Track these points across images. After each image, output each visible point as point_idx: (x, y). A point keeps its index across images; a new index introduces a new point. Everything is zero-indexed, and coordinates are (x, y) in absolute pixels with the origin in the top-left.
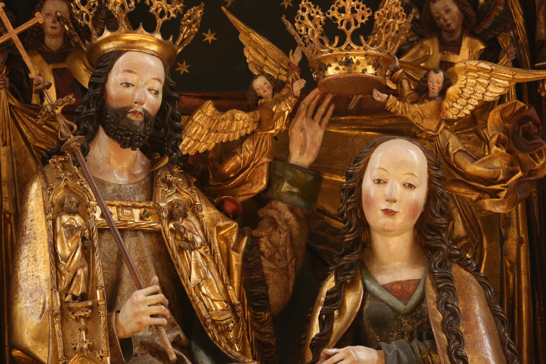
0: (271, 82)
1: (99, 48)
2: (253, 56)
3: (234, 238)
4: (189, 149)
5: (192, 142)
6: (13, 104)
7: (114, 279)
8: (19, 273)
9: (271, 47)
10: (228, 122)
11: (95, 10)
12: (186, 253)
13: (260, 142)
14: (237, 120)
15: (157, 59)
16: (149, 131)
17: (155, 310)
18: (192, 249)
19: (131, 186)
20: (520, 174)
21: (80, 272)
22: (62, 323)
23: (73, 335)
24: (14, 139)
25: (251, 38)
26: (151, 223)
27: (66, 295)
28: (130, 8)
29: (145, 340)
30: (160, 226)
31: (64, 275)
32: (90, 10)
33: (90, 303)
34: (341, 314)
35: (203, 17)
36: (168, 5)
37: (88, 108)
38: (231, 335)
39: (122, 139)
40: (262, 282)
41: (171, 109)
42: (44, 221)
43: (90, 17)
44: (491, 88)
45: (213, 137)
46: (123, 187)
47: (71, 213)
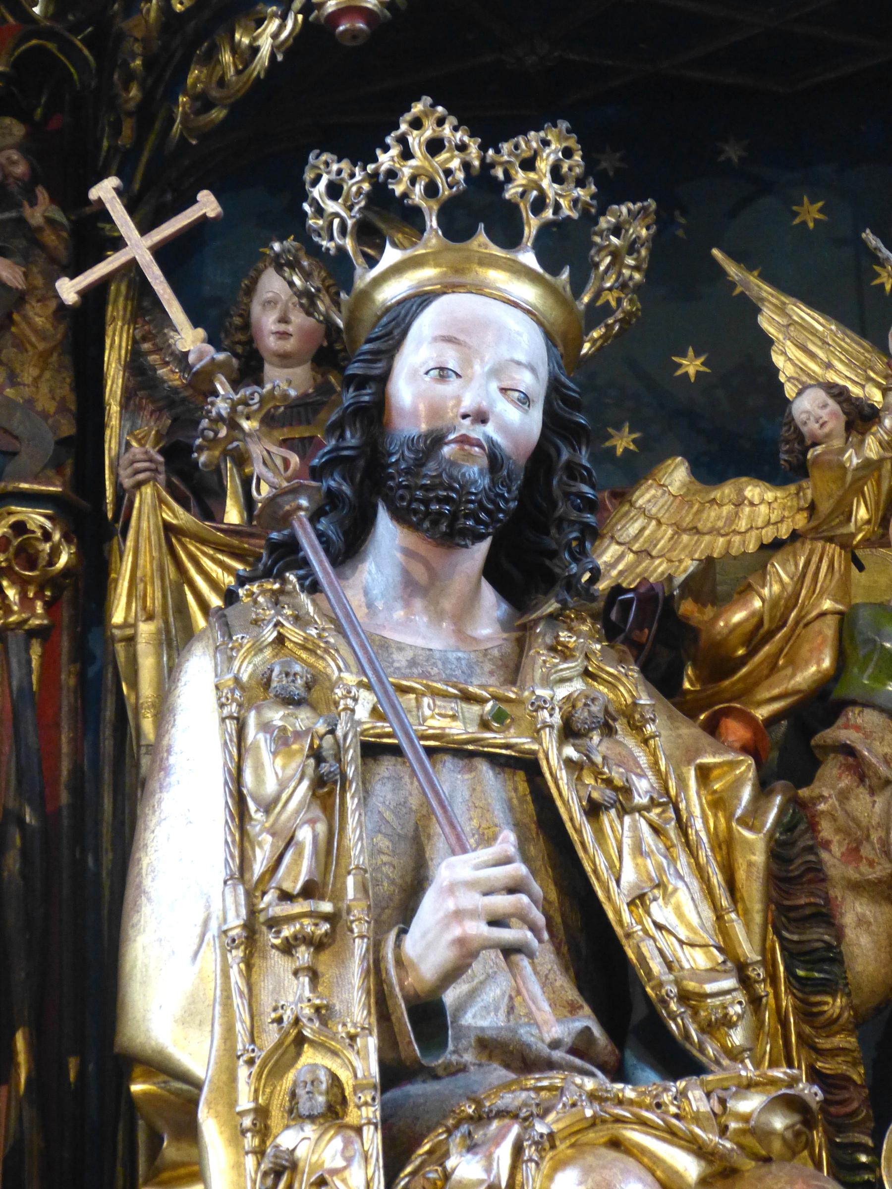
0: (839, 403)
1: (373, 301)
2: (795, 365)
4: (621, 573)
5: (630, 557)
6: (174, 522)
7: (408, 879)
8: (145, 862)
9: (840, 335)
10: (727, 509)
11: (363, 204)
12: (608, 819)
13: (815, 559)
14: (752, 504)
15: (526, 318)
16: (506, 501)
17: (502, 902)
18: (624, 810)
19: (460, 654)
21: (305, 835)
22: (248, 962)
23: (277, 991)
25: (790, 317)
28: (451, 187)
29: (489, 1033)
30: (535, 747)
32: (350, 208)
33: (326, 907)
35: (656, 241)
36: (556, 186)
37: (342, 437)
38: (737, 1037)
39: (427, 513)
40: (825, 916)
41: (565, 455)
43: (350, 223)
45: (686, 547)
46: (437, 655)
47: (290, 701)
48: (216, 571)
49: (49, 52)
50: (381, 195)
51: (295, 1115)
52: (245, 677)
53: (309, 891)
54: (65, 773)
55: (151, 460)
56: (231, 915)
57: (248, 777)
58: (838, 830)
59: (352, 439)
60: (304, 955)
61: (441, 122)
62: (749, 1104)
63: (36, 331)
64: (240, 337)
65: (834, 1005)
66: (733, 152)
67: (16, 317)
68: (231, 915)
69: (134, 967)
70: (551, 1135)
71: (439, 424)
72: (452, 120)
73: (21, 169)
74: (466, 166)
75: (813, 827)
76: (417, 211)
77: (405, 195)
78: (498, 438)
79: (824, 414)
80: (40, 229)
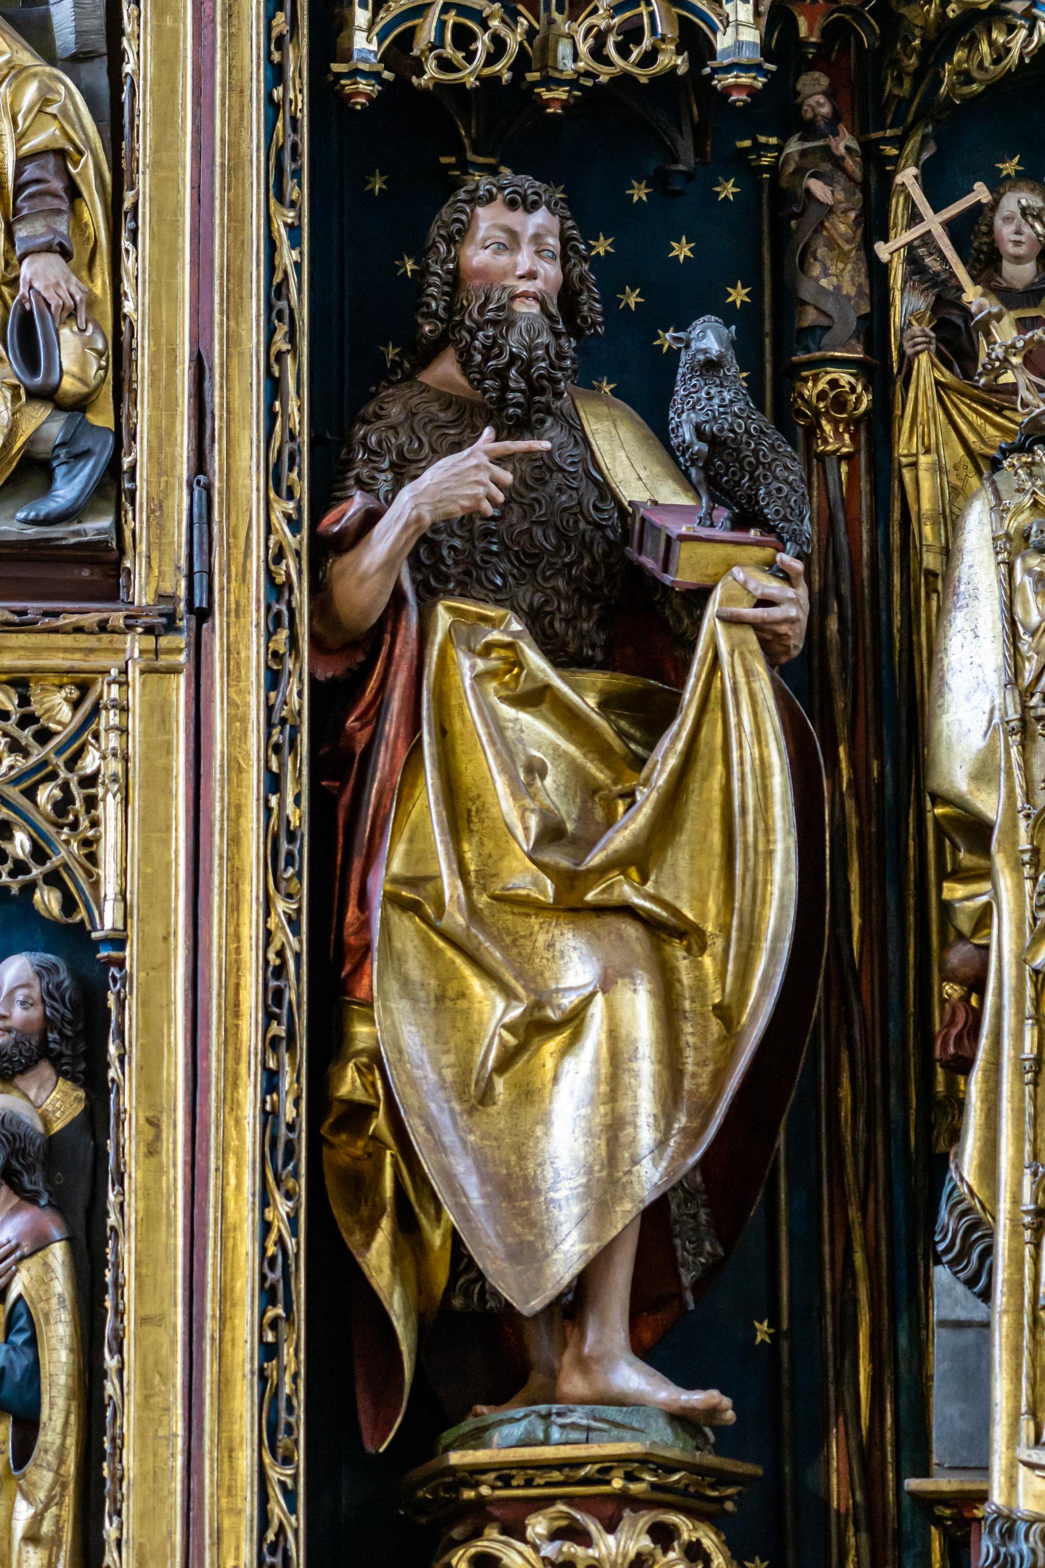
8: (946, 661)
22: (1023, 744)
24: (945, 443)
27: (1032, 695)
31: (1029, 659)
42: (993, 567)
48: (972, 417)
49: (845, 20)
52: (1012, 532)
54: (865, 554)
55: (926, 336)
56: (1011, 711)
57: (1019, 610)
63: (841, 235)
64: (985, 239)
67: (827, 224)
68: (1011, 711)
69: (940, 736)
73: (826, 110)
80: (843, 158)
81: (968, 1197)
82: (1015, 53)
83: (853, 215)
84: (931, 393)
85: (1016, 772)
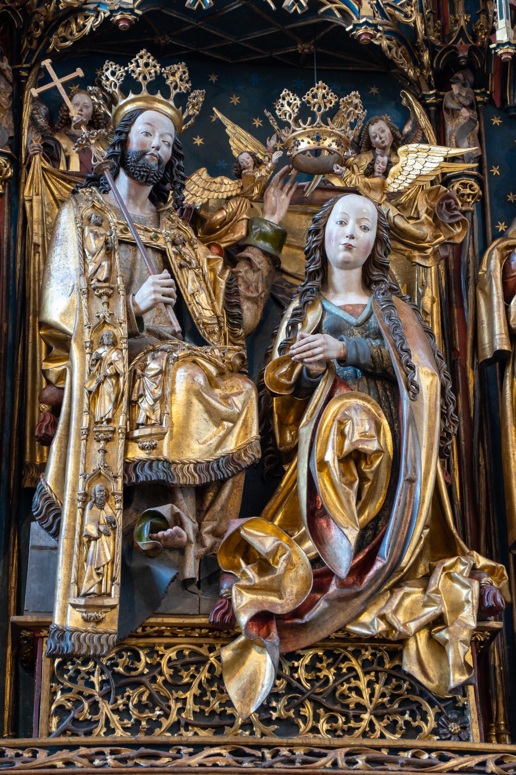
3: (220, 267)
8: (52, 266)
20: (442, 238)
22: (88, 298)
26: (161, 243)
34: (303, 327)
35: (203, 102)
40: (238, 306)
41: (177, 163)
44: (427, 165)
50: (128, 76)
51: (102, 344)
53: (106, 281)
58: (244, 282)
59: (117, 149)
60: (105, 298)
61: (149, 58)
62: (230, 355)
65: (240, 332)
66: (213, 78)
70: (178, 357)
71: (145, 149)
72: (152, 58)
74: (156, 72)
75: (237, 280)
76: (140, 84)
77: (137, 78)
78: (161, 155)
79: (248, 161)
81: (49, 492)
82: (88, 28)
83: (8, 95)
84: (40, 171)
85: (84, 310)
